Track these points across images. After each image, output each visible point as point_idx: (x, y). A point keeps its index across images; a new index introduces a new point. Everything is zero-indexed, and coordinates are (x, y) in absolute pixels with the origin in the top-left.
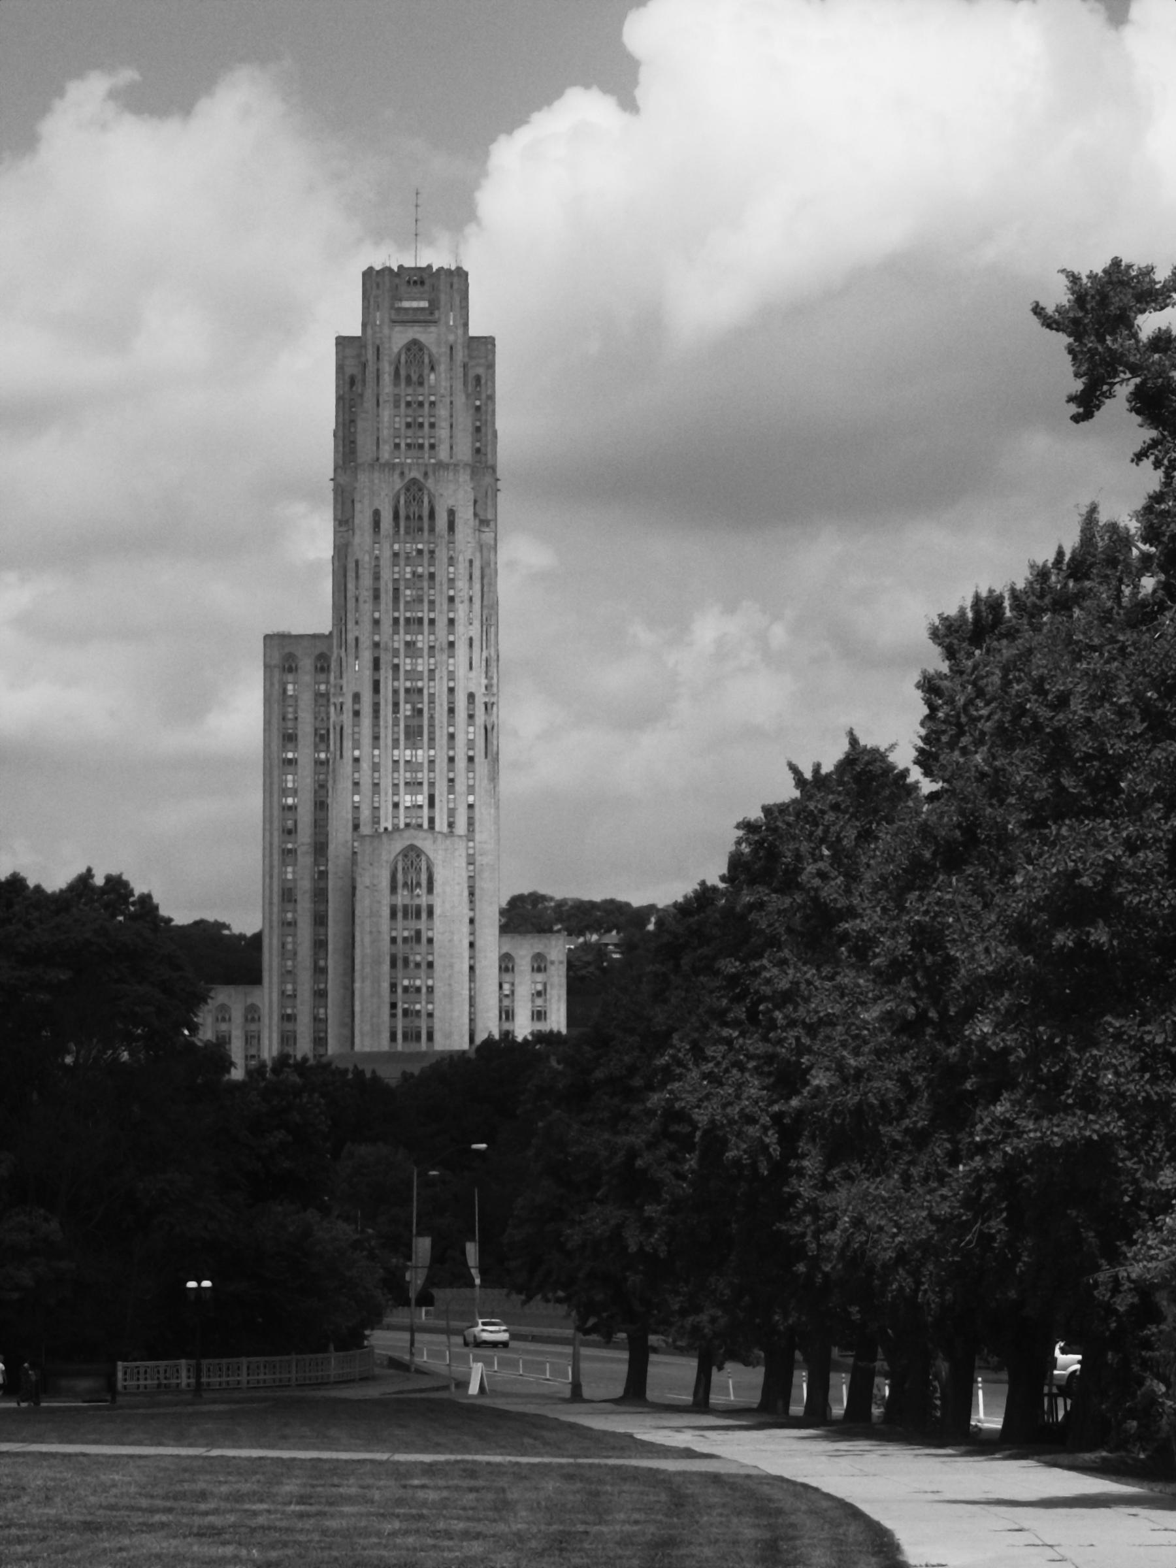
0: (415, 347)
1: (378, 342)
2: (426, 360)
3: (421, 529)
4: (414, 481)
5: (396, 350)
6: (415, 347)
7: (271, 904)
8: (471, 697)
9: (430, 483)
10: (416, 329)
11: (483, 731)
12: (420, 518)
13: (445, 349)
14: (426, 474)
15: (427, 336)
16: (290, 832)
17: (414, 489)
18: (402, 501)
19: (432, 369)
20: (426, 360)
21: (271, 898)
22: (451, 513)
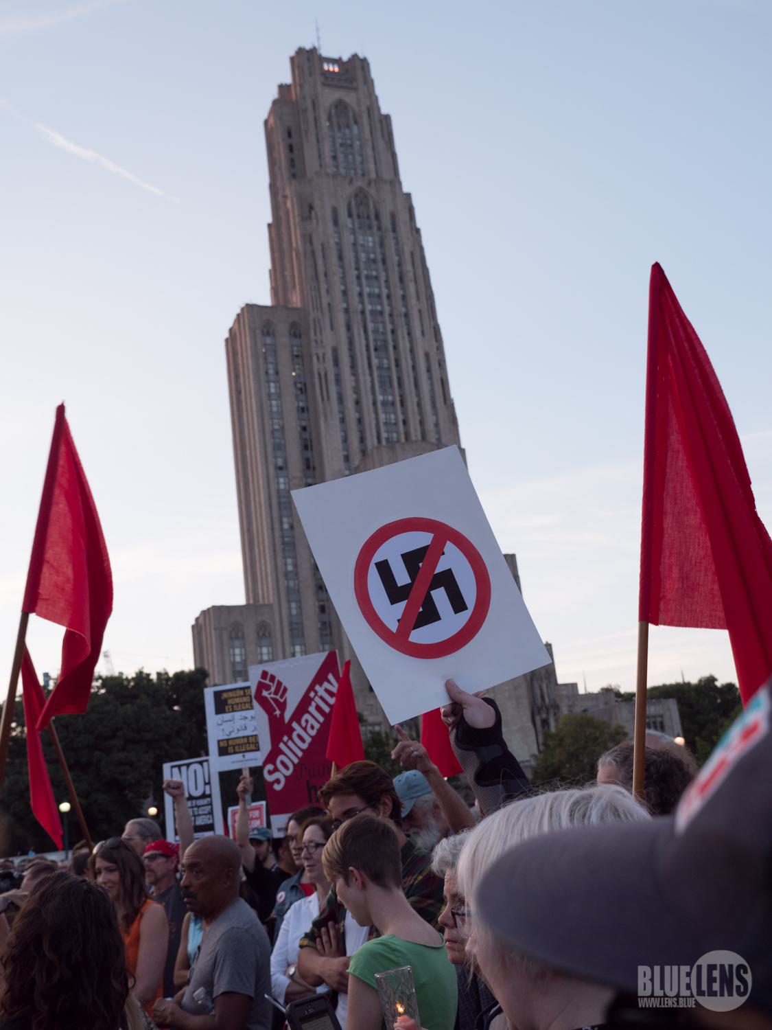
0: (341, 106)
2: (351, 115)
3: (370, 227)
4: (361, 190)
6: (341, 106)
7: (273, 529)
8: (427, 355)
9: (372, 191)
11: (440, 382)
12: (368, 217)
13: (364, 108)
14: (369, 184)
15: (350, 98)
16: (281, 468)
17: (361, 196)
18: (353, 203)
19: (356, 122)
21: (272, 524)
22: (393, 217)
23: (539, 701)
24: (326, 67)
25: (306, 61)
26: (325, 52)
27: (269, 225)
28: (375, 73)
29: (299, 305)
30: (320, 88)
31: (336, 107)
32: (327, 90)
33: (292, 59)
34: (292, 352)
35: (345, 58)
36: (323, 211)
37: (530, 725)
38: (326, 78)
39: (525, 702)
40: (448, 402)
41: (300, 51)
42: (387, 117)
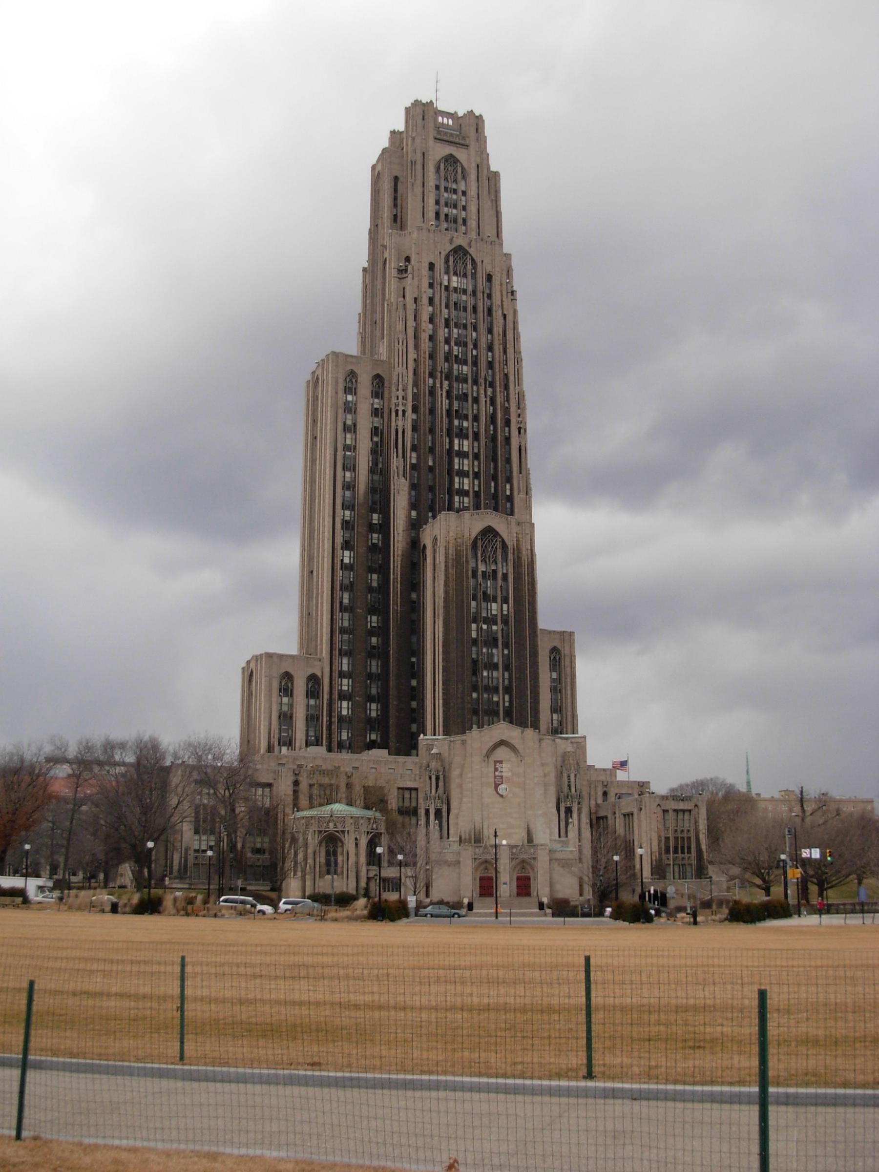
0: (451, 160)
1: (424, 150)
2: (459, 170)
5: (438, 158)
6: (451, 160)
10: (452, 148)
13: (474, 165)
15: (461, 155)
20: (459, 170)
23: (566, 789)
24: (440, 119)
25: (421, 113)
26: (441, 106)
27: (365, 270)
28: (489, 131)
29: (384, 357)
30: (431, 142)
31: (446, 160)
32: (439, 145)
33: (407, 110)
34: (372, 404)
35: (460, 114)
36: (419, 264)
37: (554, 810)
38: (439, 132)
39: (552, 790)
40: (524, 472)
41: (417, 103)
42: (496, 175)
